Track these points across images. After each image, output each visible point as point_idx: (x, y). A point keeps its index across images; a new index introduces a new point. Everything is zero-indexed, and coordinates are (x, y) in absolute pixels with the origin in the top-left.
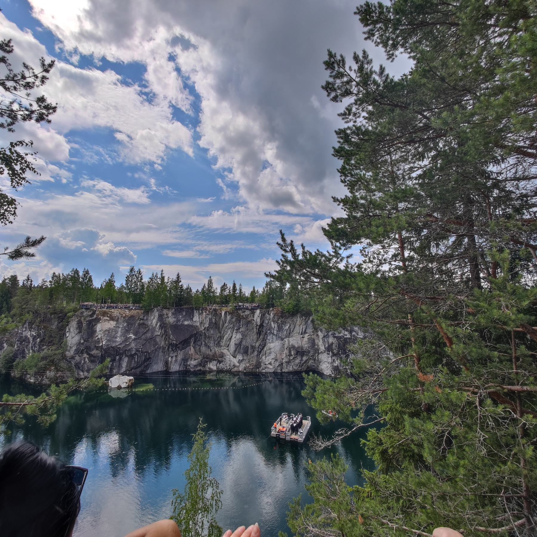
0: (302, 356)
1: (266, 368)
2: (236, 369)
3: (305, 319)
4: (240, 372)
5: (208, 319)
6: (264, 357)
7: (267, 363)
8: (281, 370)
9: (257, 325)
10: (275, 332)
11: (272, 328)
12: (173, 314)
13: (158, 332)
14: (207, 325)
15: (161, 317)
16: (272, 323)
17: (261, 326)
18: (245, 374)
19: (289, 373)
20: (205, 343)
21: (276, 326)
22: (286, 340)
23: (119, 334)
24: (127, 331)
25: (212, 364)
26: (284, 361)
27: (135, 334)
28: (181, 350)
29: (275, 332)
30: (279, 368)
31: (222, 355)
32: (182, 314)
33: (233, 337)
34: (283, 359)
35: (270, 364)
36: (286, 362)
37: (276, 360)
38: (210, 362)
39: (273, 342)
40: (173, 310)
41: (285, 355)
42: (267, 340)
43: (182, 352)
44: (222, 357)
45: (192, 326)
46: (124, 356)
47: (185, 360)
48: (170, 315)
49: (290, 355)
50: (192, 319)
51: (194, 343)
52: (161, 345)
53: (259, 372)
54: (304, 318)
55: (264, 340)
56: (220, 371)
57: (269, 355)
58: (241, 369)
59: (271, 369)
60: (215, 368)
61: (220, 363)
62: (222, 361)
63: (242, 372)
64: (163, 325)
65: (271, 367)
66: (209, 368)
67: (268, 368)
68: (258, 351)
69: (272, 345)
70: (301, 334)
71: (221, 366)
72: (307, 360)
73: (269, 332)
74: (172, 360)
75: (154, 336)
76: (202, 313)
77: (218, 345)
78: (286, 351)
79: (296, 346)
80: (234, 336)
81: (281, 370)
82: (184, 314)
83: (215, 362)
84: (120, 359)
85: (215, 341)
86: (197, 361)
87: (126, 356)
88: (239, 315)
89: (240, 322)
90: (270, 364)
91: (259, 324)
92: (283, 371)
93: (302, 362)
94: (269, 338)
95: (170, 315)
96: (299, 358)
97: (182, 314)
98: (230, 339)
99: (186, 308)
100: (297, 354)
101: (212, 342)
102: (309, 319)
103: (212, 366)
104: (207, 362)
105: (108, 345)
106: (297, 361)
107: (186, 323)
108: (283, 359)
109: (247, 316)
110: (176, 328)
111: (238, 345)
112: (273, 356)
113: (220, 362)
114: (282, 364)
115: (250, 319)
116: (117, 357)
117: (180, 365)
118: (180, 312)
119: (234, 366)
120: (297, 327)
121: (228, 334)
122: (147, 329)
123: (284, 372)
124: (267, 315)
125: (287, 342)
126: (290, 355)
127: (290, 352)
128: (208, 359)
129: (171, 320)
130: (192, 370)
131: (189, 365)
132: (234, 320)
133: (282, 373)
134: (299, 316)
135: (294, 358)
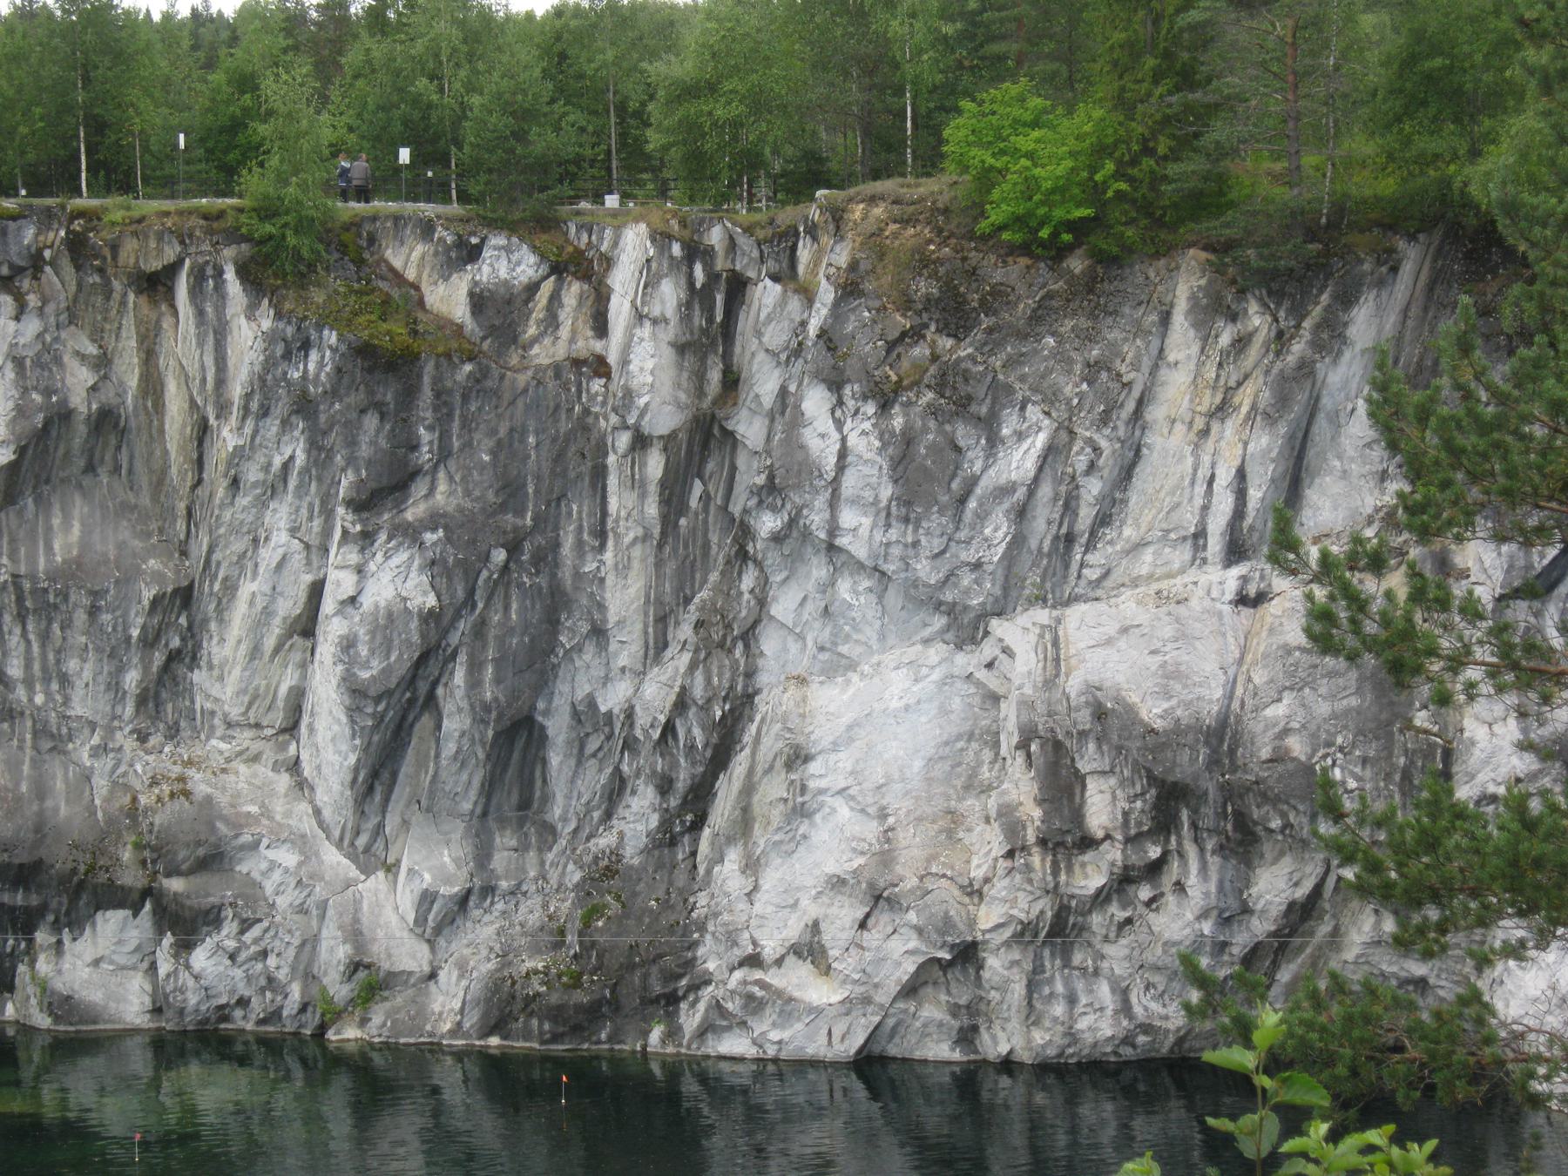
0: (1242, 844)
1: (754, 1005)
3: (1281, 339)
6: (729, 873)
7: (771, 948)
8: (967, 1037)
9: (641, 442)
10: (859, 529)
11: (806, 469)
16: (815, 402)
17: (705, 438)
18: (502, 1078)
19: (1071, 1074)
21: (862, 437)
22: (1018, 633)
26: (988, 916)
29: (859, 529)
30: (932, 1010)
33: (328, 605)
34: (975, 892)
35: (810, 949)
36: (1025, 934)
37: (880, 899)
38: (74, 921)
39: (838, 666)
41: (998, 847)
42: (769, 642)
44: (213, 860)
49: (1067, 839)
53: (674, 1069)
54: (1256, 319)
55: (733, 637)
57: (793, 843)
59: (818, 1016)
60: (130, 1004)
61: (185, 946)
62: (211, 917)
63: (459, 1055)
65: (820, 992)
66: (62, 1006)
67: (788, 1006)
68: (665, 786)
69: (831, 706)
70: (1236, 551)
72: (1302, 913)
73: (768, 523)
77: (164, 696)
78: (1020, 787)
79: (1153, 712)
80: (340, 583)
81: (967, 1037)
83: (115, 930)
90: (810, 949)
91: (664, 418)
92: (1000, 1041)
93: (1241, 941)
94: (783, 606)
96: (1197, 880)
98: (306, 626)
100: (1163, 824)
102: (1331, 337)
104: (25, 922)
106: (1179, 919)
108: (975, 892)
109: (500, 311)
112: (834, 843)
113: (185, 925)
114: (968, 954)
115: (545, 353)
119: (372, 982)
120: (1168, 448)
121: (268, 556)
123: (1008, 1065)
124: (766, 294)
125: (1026, 665)
126: (1067, 839)
127: (1062, 787)
132: (318, 365)
133: (969, 1081)
134: (1186, 284)
135: (1124, 881)
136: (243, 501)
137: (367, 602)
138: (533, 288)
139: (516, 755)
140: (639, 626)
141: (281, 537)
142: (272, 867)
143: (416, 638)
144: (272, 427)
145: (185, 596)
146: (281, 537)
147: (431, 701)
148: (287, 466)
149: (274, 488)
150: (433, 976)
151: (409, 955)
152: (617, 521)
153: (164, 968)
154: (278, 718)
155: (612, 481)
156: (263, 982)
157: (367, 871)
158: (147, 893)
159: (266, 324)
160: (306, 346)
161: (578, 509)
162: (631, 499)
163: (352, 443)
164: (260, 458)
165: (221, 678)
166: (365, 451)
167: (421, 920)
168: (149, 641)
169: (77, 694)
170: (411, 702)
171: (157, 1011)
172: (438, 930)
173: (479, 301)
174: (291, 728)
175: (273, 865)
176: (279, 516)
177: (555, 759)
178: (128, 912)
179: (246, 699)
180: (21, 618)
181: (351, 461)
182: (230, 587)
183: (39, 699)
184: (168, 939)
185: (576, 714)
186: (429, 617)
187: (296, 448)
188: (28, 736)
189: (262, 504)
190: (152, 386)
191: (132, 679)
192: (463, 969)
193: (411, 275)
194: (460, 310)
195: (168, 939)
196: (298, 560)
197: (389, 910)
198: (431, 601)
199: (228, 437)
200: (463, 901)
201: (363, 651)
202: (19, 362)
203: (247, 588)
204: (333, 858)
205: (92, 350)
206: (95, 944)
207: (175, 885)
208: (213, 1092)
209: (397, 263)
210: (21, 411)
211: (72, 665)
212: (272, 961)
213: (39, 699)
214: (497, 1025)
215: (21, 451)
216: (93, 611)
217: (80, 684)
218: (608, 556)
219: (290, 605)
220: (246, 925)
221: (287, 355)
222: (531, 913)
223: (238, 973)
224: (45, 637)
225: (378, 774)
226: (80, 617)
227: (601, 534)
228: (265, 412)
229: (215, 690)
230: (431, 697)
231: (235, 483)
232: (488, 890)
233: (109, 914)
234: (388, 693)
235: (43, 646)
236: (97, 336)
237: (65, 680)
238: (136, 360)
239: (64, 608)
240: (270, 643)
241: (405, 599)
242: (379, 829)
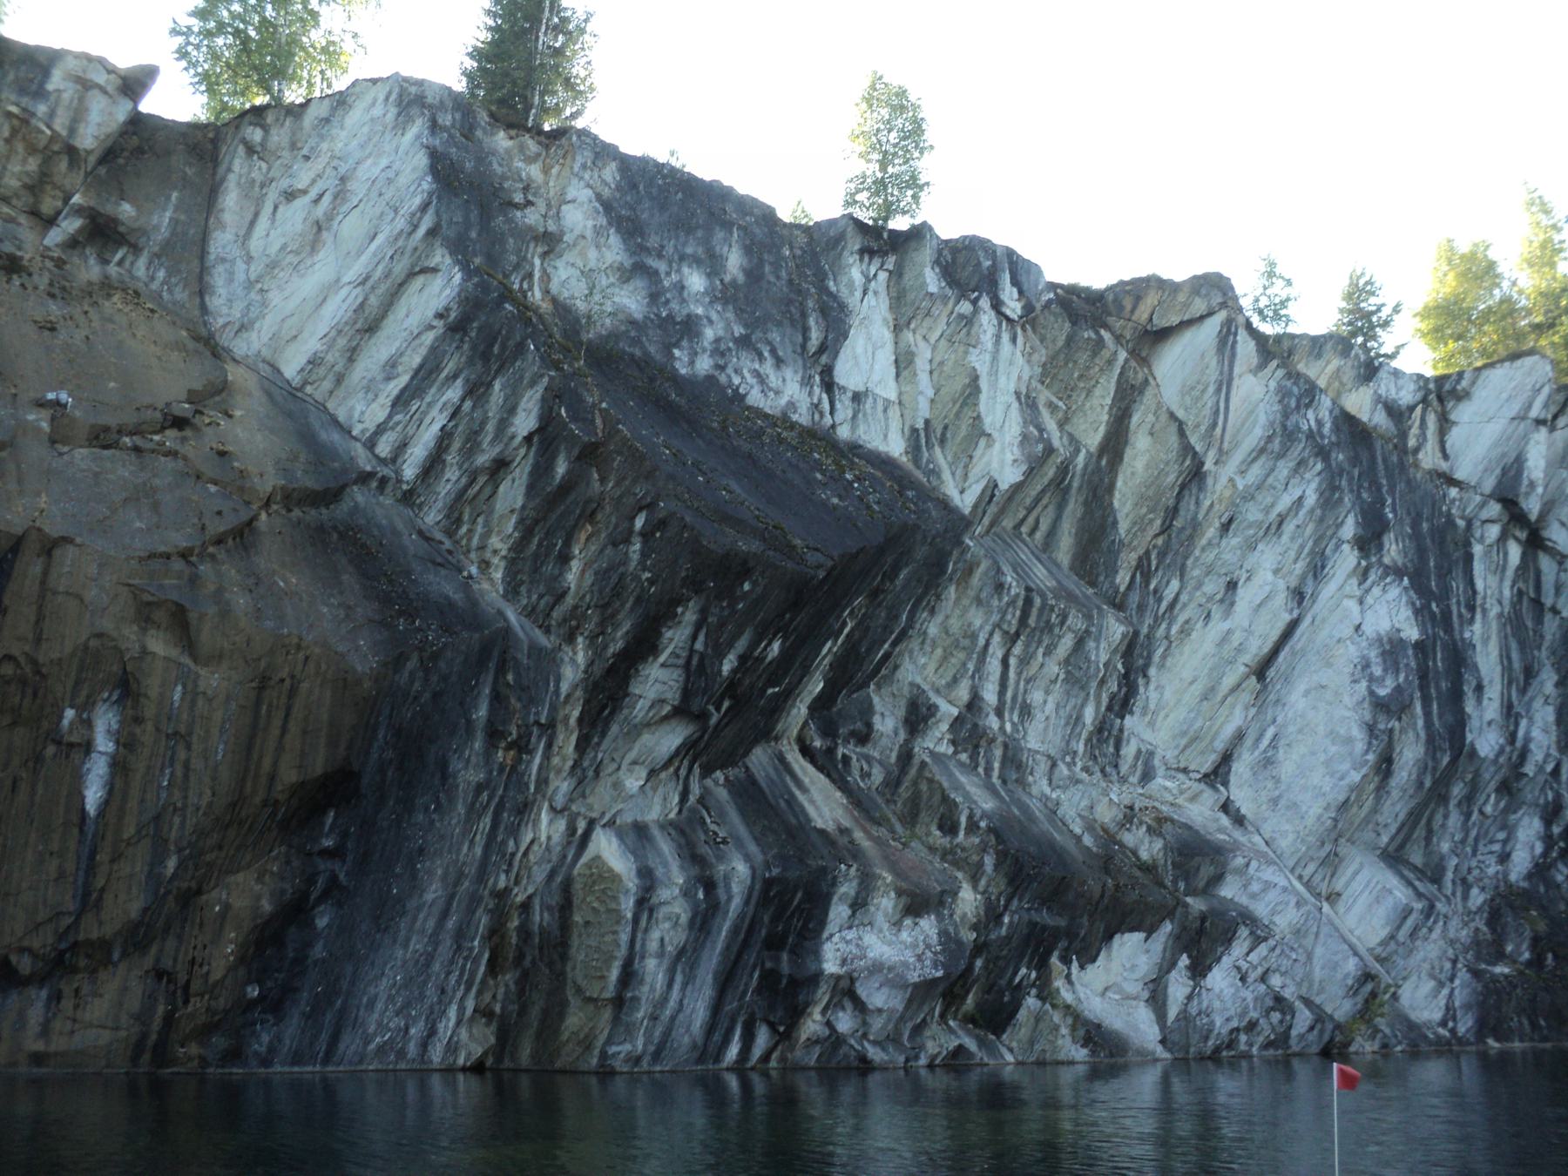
61: (1199, 970)
74: (648, 879)
83: (1130, 957)
97: (712, 264)
113: (1202, 942)
118: (682, 226)
121: (1246, 597)
131: (846, 992)
136: (1233, 541)
137: (1368, 629)
138: (1412, 409)
140: (1499, 687)
141: (1265, 576)
142: (1262, 888)
146: (1265, 576)
152: (1485, 598)
154: (1207, 767)
155: (1478, 568)
156: (1269, 1002)
161: (1458, 586)
162: (1493, 581)
165: (1152, 724)
174: (1218, 774)
176: (1267, 558)
178: (1142, 935)
179: (1184, 742)
182: (1185, 631)
188: (996, 765)
189: (1251, 546)
190: (1115, 443)
191: (1089, 714)
201: (1377, 671)
206: (1108, 971)
211: (1036, 696)
217: (1039, 716)
219: (1258, 647)
220: (1257, 940)
226: (1066, 643)
228: (1281, 455)
229: (1147, 735)
233: (1127, 935)
235: (1019, 674)
236: (1067, 392)
237: (1026, 711)
238: (1106, 417)
239: (1057, 630)
240: (1229, 681)
241: (1399, 631)
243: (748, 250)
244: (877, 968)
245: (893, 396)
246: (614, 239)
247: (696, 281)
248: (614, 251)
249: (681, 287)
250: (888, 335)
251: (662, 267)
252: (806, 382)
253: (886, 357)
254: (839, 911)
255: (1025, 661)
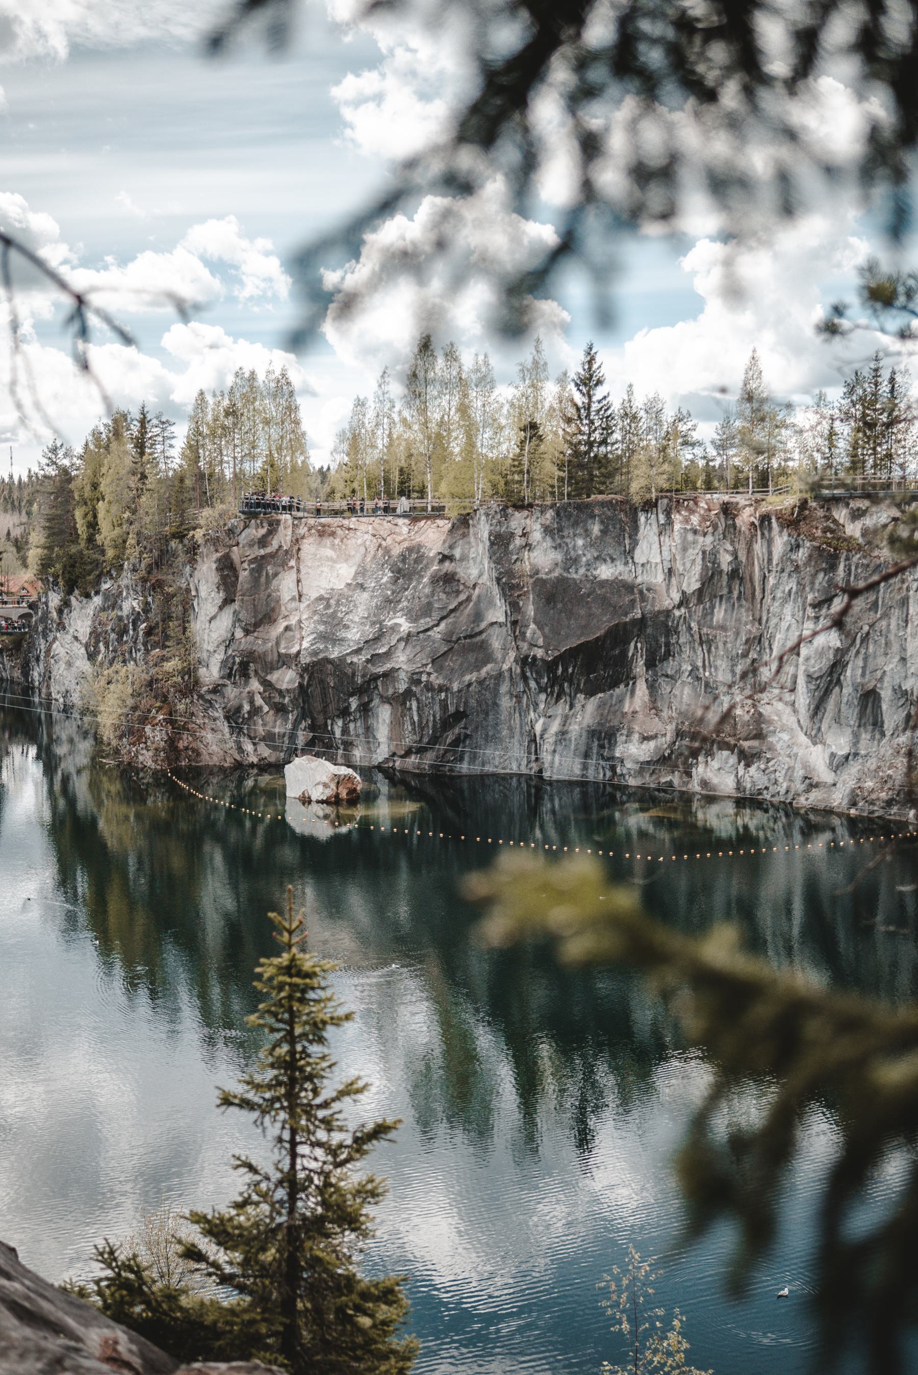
2: (814, 798)
4: (829, 812)
5: (694, 553)
12: (547, 530)
13: (498, 613)
14: (692, 584)
15: (500, 542)
18: (853, 825)
20: (695, 668)
23: (361, 612)
24: (390, 603)
25: (715, 764)
27: (414, 618)
28: (590, 693)
31: (759, 730)
32: (587, 533)
40: (550, 514)
43: (592, 704)
44: (759, 736)
45: (629, 588)
46: (376, 701)
47: (603, 737)
48: (537, 535)
50: (629, 554)
51: (651, 664)
52: (505, 667)
56: (747, 801)
58: (838, 799)
61: (748, 765)
63: (840, 815)
64: (509, 586)
66: (704, 783)
71: (753, 776)
75: (483, 625)
76: (670, 522)
82: (596, 529)
84: (365, 709)
85: (733, 660)
86: (652, 744)
87: (386, 700)
88: (835, 529)
89: (833, 567)
95: (537, 535)
97: (587, 533)
99: (602, 504)
101: (723, 664)
103: (719, 772)
104: (695, 754)
105: (315, 653)
107: (605, 572)
110: (556, 594)
111: (829, 680)
113: (747, 758)
116: (354, 703)
117: (587, 755)
118: (575, 524)
119: (812, 786)
121: (784, 625)
122: (462, 597)
128: (696, 742)
129: (542, 558)
130: (632, 782)
132: (802, 555)
136: (776, 604)
139: (870, 705)
141: (789, 618)
142: (779, 740)
143: (831, 657)
144: (785, 574)
145: (760, 639)
147: (839, 682)
148: (790, 591)
149: (785, 601)
150: (834, 785)
151: (825, 775)
153: (741, 773)
154: (789, 684)
157: (815, 744)
158: (735, 745)
159: (786, 538)
160: (798, 546)
163: (812, 583)
164: (781, 588)
166: (817, 586)
167: (831, 763)
168: (745, 655)
169: (720, 673)
170: (831, 681)
171: (738, 789)
172: (837, 767)
173: (865, 533)
175: (780, 739)
176: (788, 610)
177: (884, 707)
180: (701, 644)
181: (812, 589)
183: (707, 674)
184: (742, 763)
185: (894, 690)
186: (838, 650)
187: (792, 584)
189: (782, 606)
191: (739, 669)
192: (844, 783)
193: (841, 521)
194: (858, 534)
195: (742, 763)
196: (794, 626)
197: (817, 758)
198: (839, 644)
199: (772, 581)
200: (847, 758)
201: (813, 661)
202: (704, 552)
203: (778, 636)
204: (803, 739)
205: (730, 548)
207: (746, 744)
208: (752, 820)
209: (837, 517)
210: (705, 568)
211: (719, 662)
212: (777, 774)
213: (707, 674)
214: (854, 804)
215: (703, 584)
216: (725, 643)
218: (909, 630)
221: (791, 550)
222: (872, 764)
223: (766, 778)
224: (709, 651)
225: (817, 709)
226: (721, 645)
227: (906, 622)
228: (783, 571)
230: (839, 681)
231: (774, 598)
232: (856, 754)
234: (821, 677)
236: (732, 543)
242: (819, 729)
243: (602, 522)
244: (630, 755)
245: (659, 560)
246: (548, 539)
247: (580, 542)
248: (549, 542)
249: (574, 546)
250: (656, 538)
251: (568, 540)
252: (626, 563)
253: (656, 546)
254: (621, 739)
255: (709, 651)
